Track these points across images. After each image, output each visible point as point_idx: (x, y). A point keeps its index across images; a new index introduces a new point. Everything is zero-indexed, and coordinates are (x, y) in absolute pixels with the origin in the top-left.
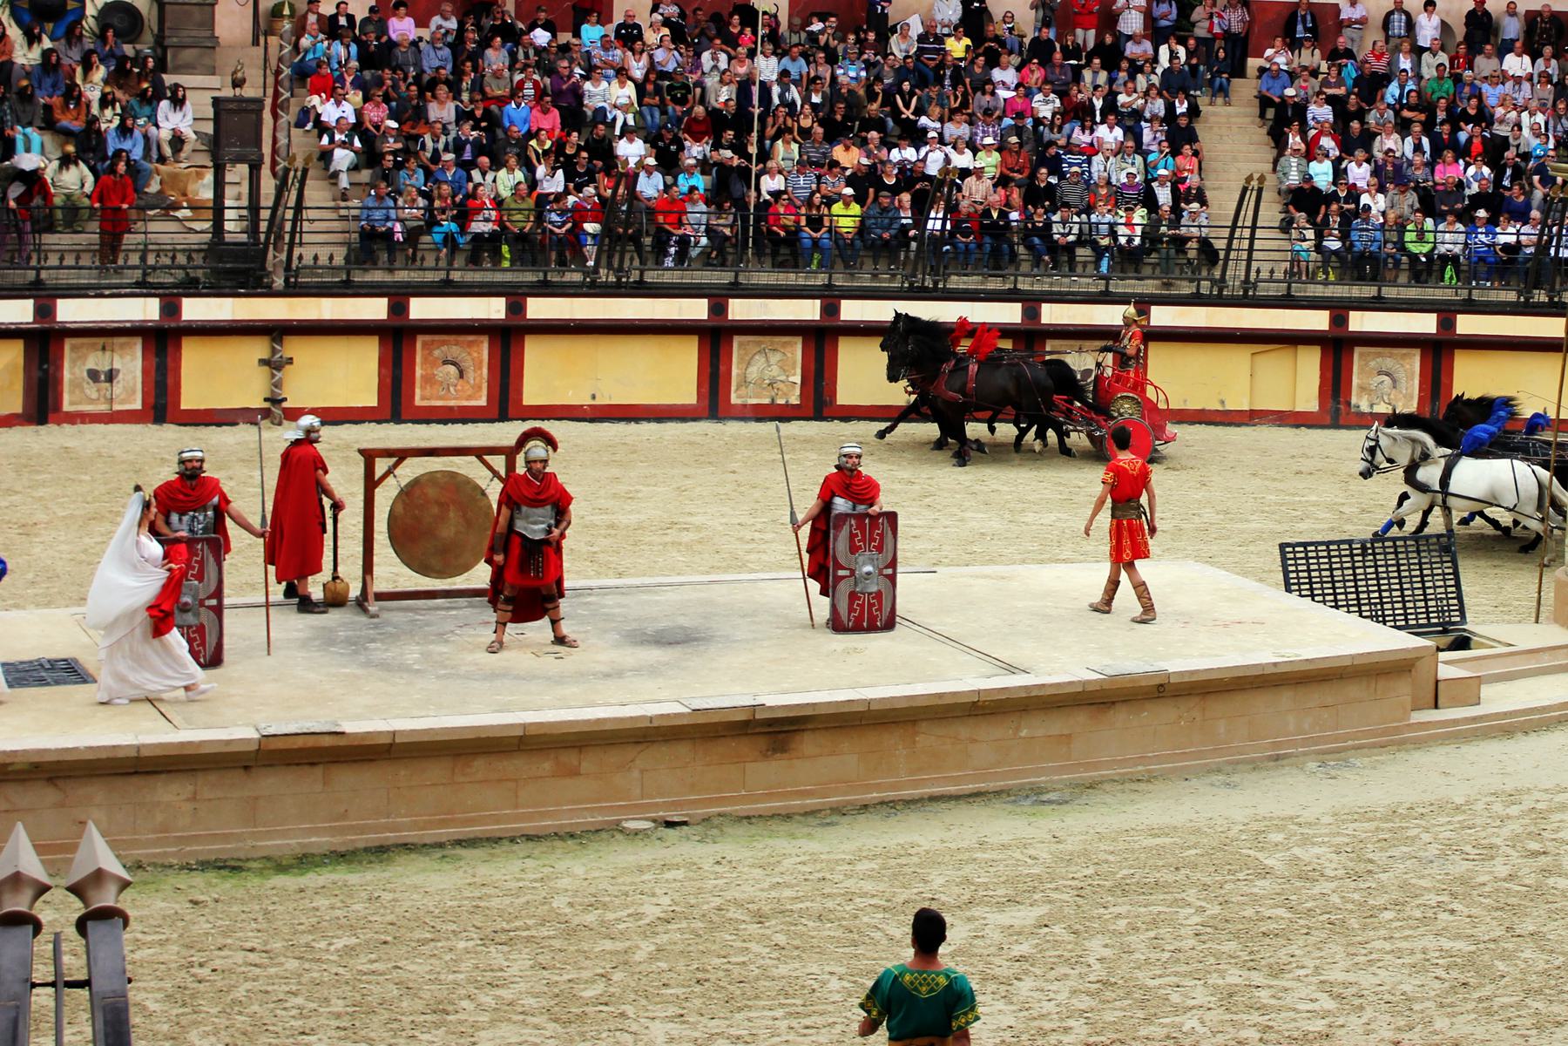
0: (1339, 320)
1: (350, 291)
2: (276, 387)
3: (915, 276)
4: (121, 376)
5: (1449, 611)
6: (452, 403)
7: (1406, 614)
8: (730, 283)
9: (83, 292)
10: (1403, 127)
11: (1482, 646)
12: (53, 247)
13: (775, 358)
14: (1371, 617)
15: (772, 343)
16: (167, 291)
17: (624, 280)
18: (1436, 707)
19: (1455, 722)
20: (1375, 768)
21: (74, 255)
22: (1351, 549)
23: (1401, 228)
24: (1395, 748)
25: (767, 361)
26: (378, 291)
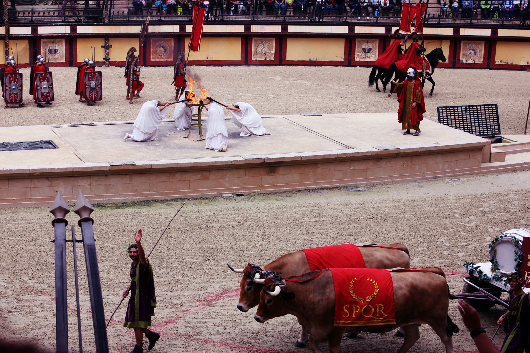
0: (457, 31)
1: (129, 24)
2: (107, 55)
3: (313, 17)
4: (58, 51)
5: (495, 130)
6: (162, 60)
7: (480, 131)
8: (251, 20)
9: (46, 24)
11: (505, 142)
12: (21, 10)
13: (266, 45)
14: (468, 132)
15: (265, 40)
16: (72, 24)
17: (217, 19)
18: (490, 162)
20: (469, 182)
21: (53, 12)
22: (462, 109)
24: (476, 175)
25: (264, 46)
26: (134, 23)
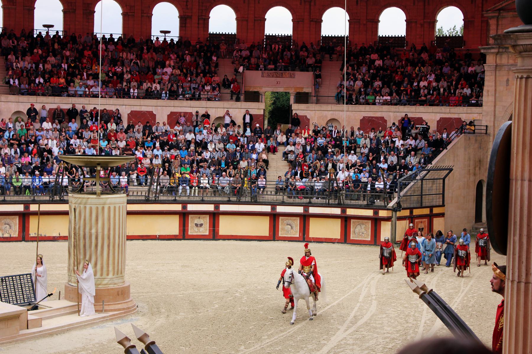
5: (31, 298)
7: (17, 300)
10: (11, 146)
11: (42, 308)
18: (28, 328)
19: (34, 333)
20: (8, 350)
23: (11, 178)
